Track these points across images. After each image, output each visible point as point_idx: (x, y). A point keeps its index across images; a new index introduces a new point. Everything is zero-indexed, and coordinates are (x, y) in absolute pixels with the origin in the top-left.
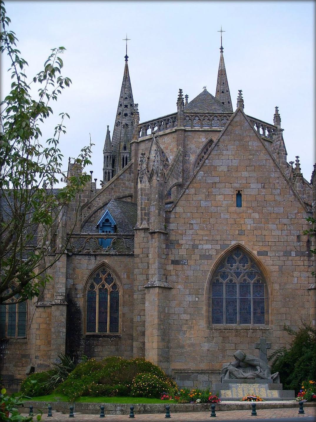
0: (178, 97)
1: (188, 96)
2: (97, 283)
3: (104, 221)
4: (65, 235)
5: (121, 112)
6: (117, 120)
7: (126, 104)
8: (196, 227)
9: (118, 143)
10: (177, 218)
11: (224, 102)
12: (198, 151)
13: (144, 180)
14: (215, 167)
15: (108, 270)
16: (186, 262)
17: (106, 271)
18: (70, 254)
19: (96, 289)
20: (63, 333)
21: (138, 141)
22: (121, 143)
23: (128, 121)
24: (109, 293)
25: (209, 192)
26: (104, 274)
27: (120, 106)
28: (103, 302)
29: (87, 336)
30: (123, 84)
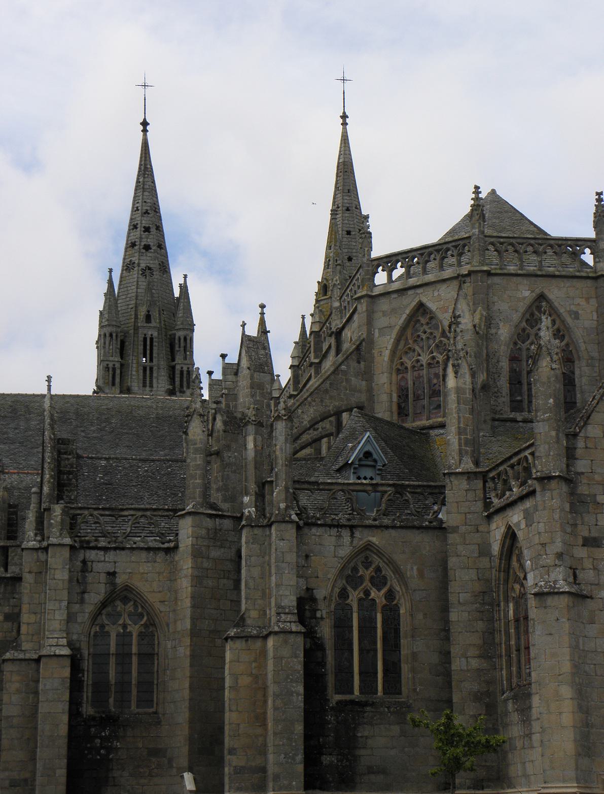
0: (472, 202)
2: (352, 588)
3: (361, 456)
4: (290, 483)
5: (135, 242)
6: (127, 257)
7: (147, 225)
9: (130, 307)
10: (590, 448)
11: (351, 230)
12: (516, 317)
13: (461, 371)
15: (376, 561)
17: (370, 562)
18: (301, 523)
19: (352, 601)
20: (298, 694)
21: (374, 294)
22: (140, 308)
23: (151, 262)
24: (379, 609)
26: (367, 568)
27: (133, 229)
28: (367, 629)
29: (339, 702)
30: (138, 182)
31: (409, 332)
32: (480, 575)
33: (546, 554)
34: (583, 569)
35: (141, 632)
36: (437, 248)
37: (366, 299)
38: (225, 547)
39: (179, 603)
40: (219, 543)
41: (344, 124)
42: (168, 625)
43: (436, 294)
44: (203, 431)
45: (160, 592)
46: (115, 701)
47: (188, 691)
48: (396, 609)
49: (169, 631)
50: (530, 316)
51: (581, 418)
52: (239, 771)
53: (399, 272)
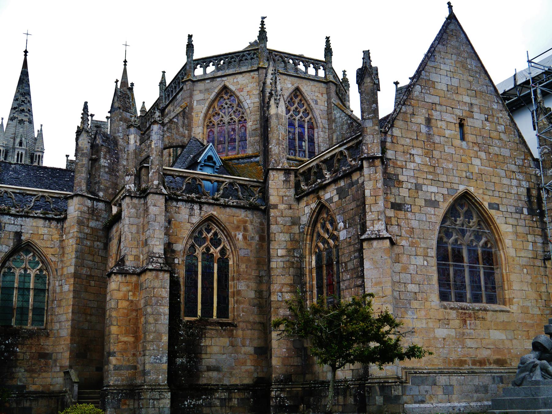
0: (260, 29)
3: (206, 158)
8: (418, 160)
14: (434, 83)
19: (198, 254)
20: (165, 315)
25: (429, 115)
26: (208, 233)
31: (216, 104)
32: (292, 237)
33: (371, 212)
34: (392, 225)
35: (37, 274)
36: (237, 54)
37: (190, 82)
38: (99, 221)
39: (66, 256)
40: (95, 218)
41: (125, 65)
42: (56, 271)
43: (235, 81)
44: (89, 142)
45: (52, 248)
46: (28, 314)
47: (71, 315)
48: (227, 260)
49: (57, 275)
51: (389, 122)
52: (116, 368)
53: (211, 69)
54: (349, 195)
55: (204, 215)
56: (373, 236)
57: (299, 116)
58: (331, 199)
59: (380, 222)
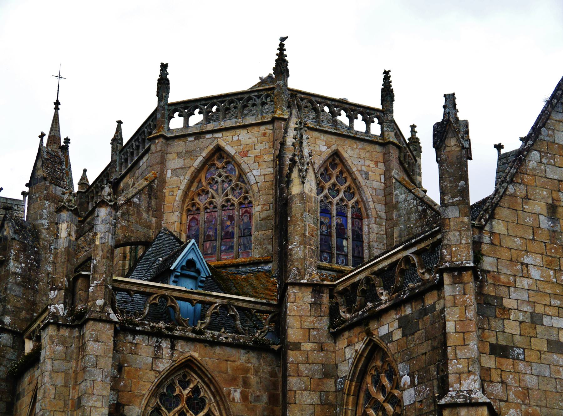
0: (277, 57)
1: (69, 140)
3: (184, 263)
8: (535, 273)
16: (520, 354)
25: (553, 199)
26: (184, 388)
32: (323, 398)
33: (456, 359)
34: (491, 382)
36: (239, 96)
37: (161, 139)
41: (57, 109)
43: (235, 138)
50: (324, 171)
51: (485, 211)
53: (196, 118)
54: (419, 330)
55: (178, 357)
56: (459, 401)
57: (338, 198)
58: (389, 335)
59: (472, 377)
